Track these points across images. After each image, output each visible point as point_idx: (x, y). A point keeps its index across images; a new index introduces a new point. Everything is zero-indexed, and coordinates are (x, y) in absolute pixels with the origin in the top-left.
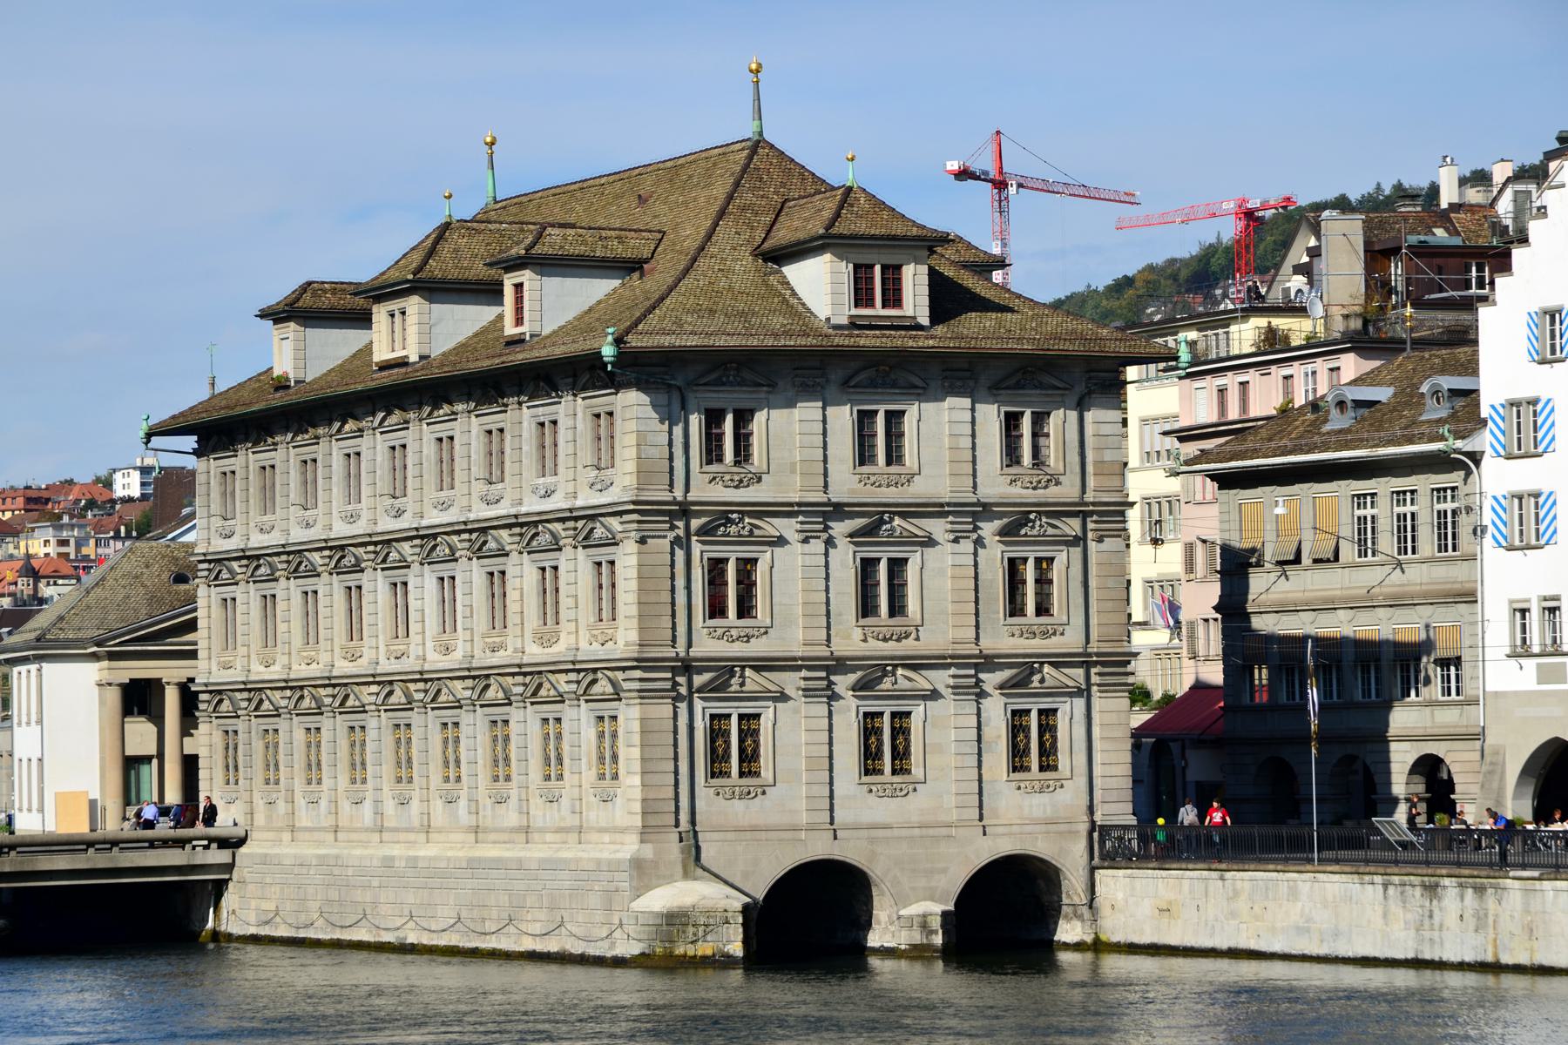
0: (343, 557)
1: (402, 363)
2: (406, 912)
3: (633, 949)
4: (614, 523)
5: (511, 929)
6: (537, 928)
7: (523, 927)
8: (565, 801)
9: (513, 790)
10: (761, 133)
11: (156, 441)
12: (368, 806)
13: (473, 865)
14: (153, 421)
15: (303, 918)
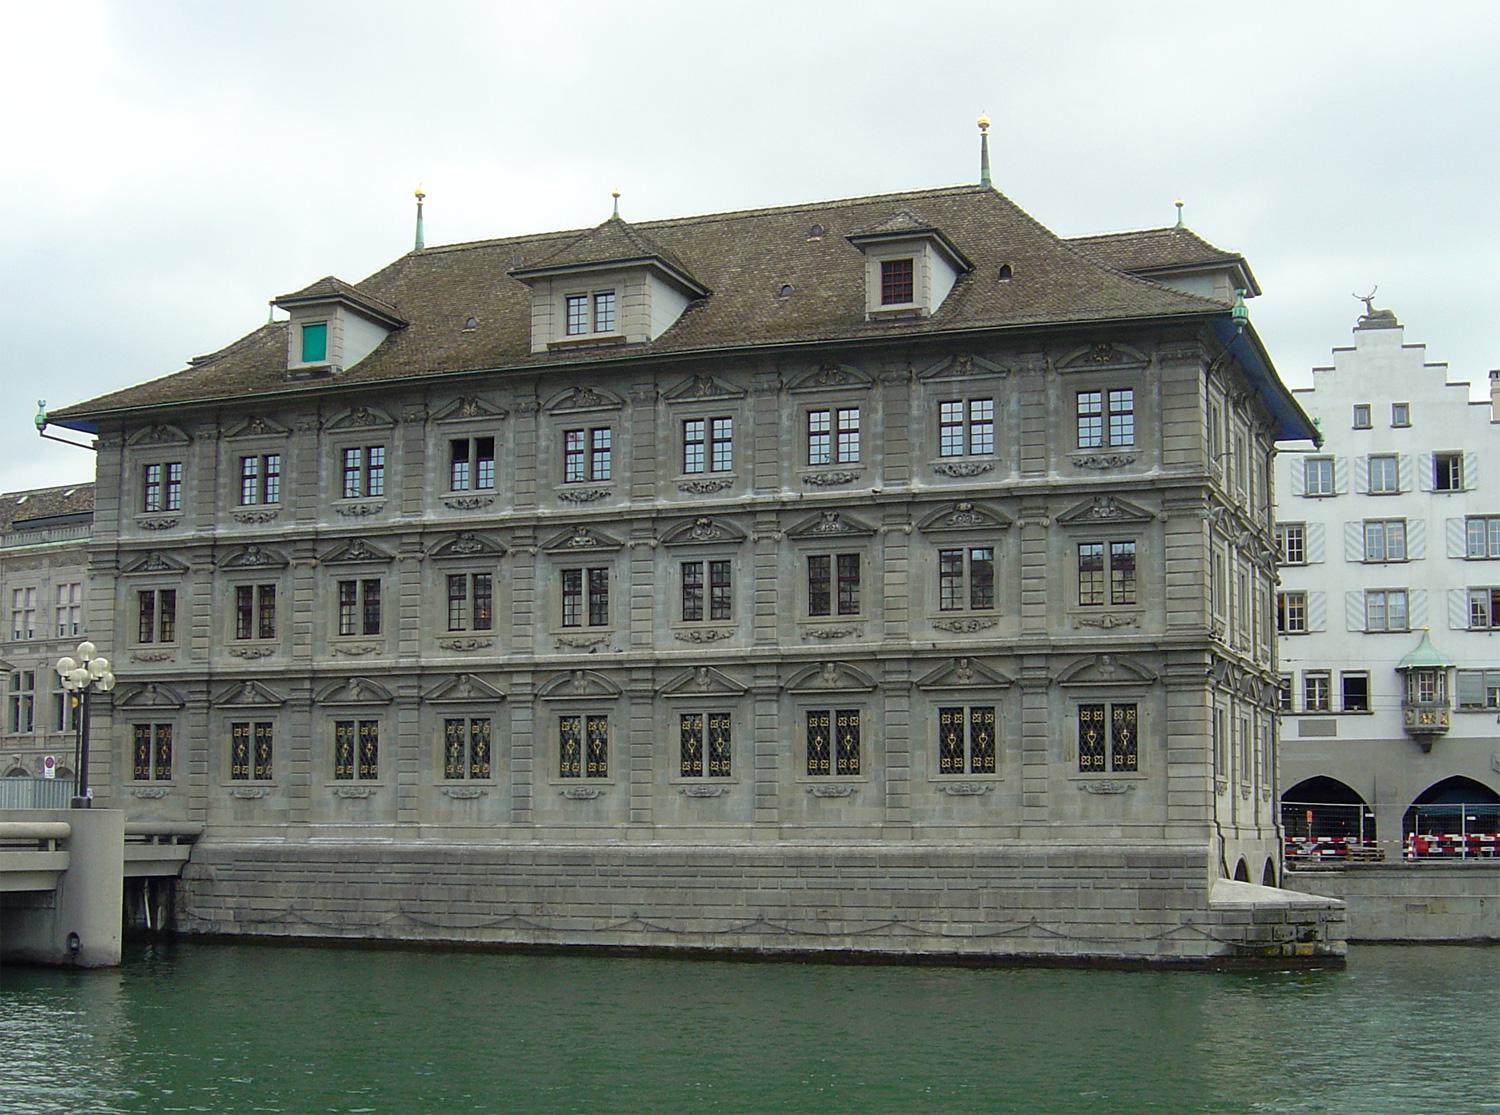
0: (455, 543)
1: (619, 342)
2: (626, 910)
3: (1215, 949)
4: (1147, 505)
5: (898, 931)
6: (967, 929)
7: (932, 928)
8: (1001, 797)
9: (868, 783)
10: (986, 180)
11: (51, 429)
12: (494, 802)
13: (799, 862)
14: (48, 409)
15: (356, 917)
